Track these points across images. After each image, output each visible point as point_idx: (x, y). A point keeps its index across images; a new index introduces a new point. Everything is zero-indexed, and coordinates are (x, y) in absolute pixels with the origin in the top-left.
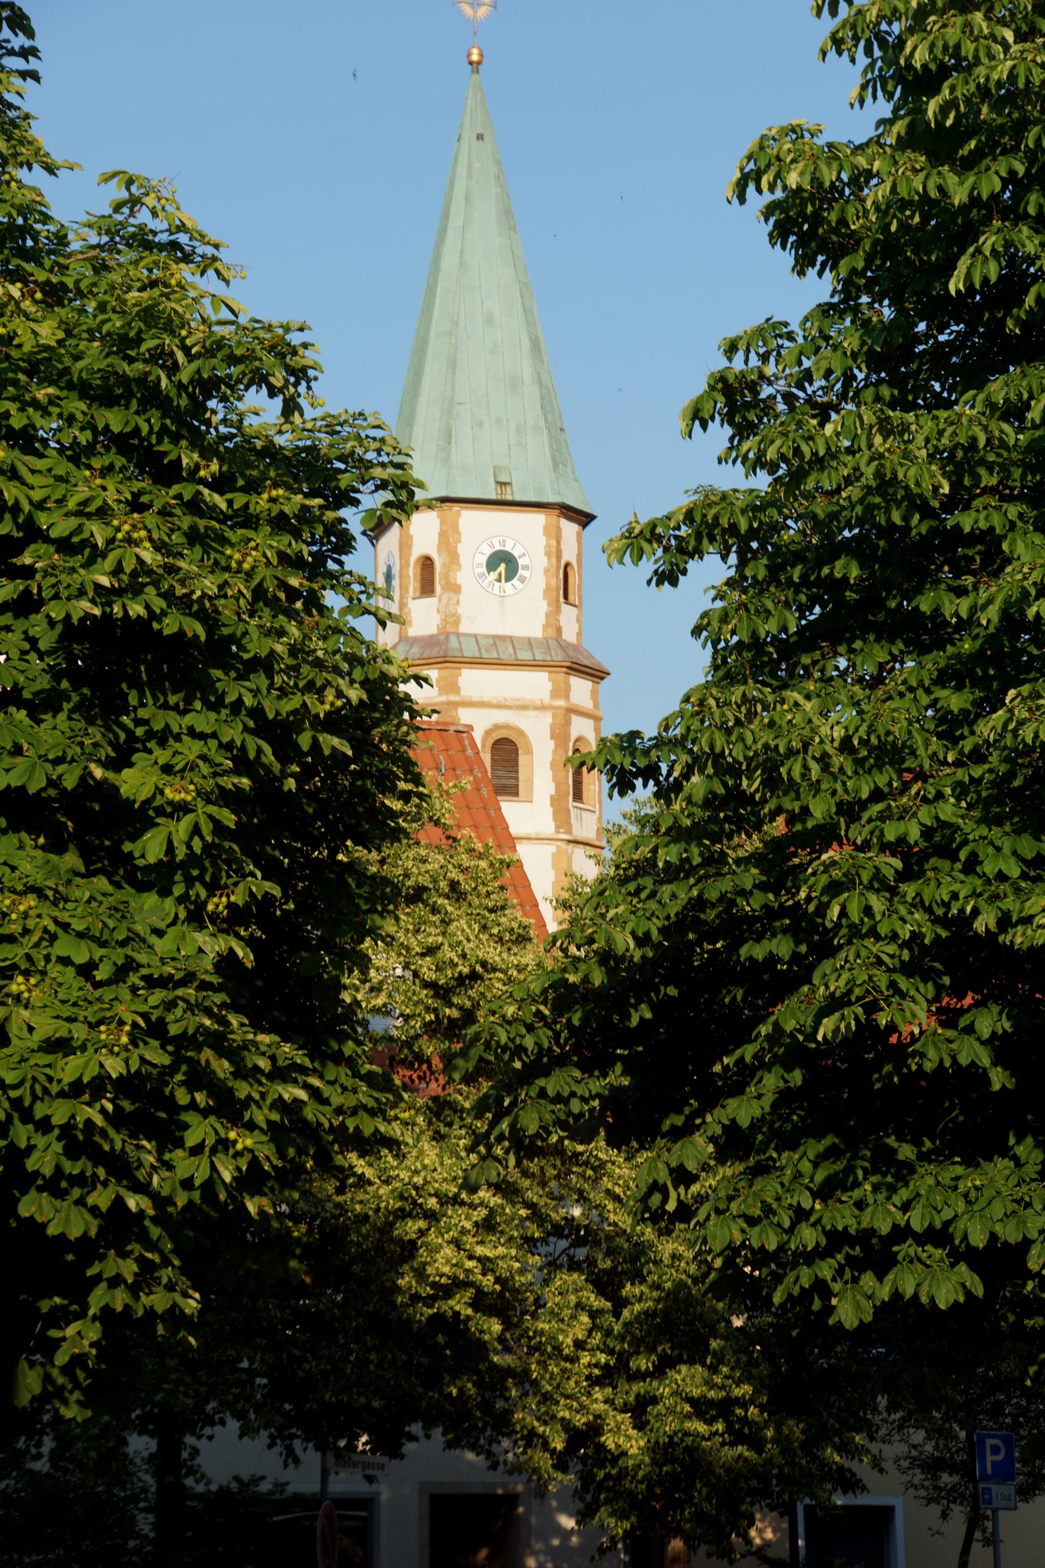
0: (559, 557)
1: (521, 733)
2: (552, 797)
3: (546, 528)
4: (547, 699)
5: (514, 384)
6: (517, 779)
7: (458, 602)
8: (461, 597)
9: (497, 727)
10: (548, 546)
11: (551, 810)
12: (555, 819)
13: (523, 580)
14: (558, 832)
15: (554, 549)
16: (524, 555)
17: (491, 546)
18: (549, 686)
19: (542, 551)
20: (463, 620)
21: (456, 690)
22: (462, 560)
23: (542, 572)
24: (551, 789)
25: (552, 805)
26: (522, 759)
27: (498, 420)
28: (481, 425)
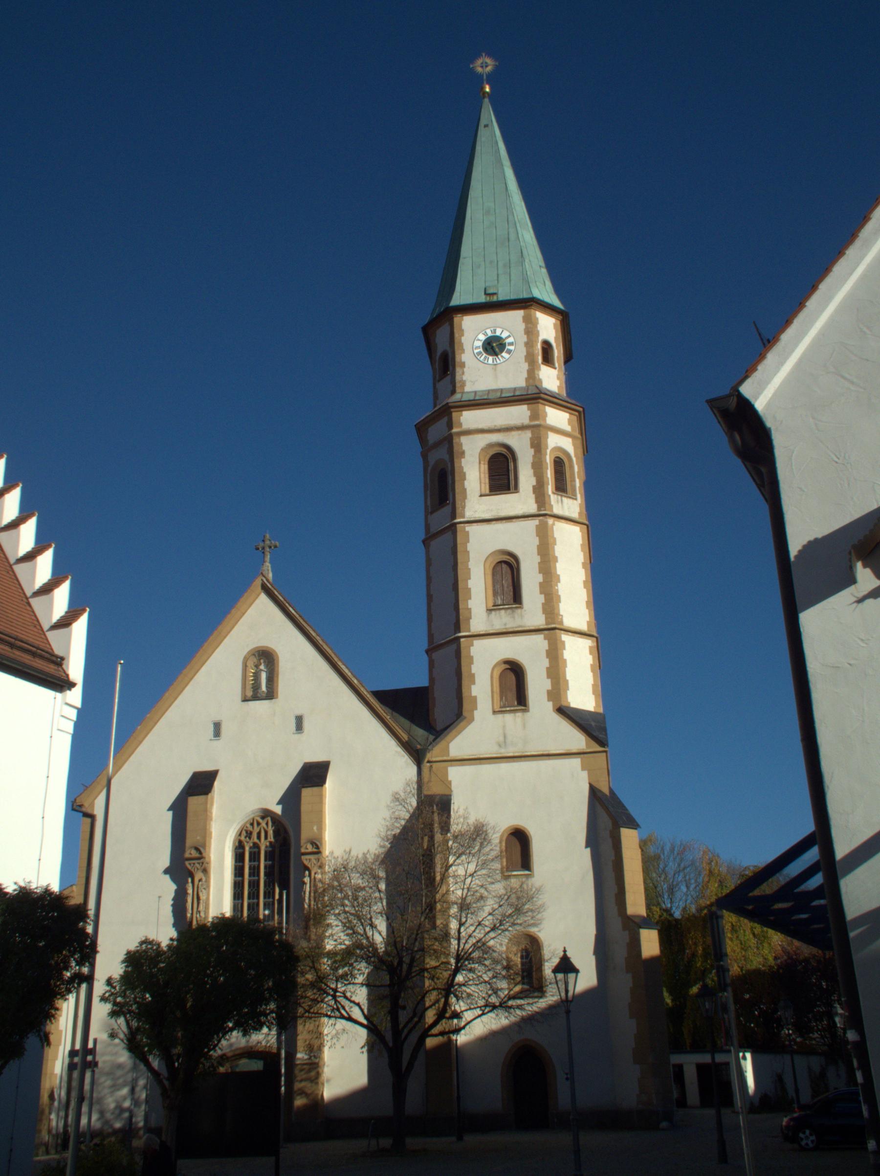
2: (534, 487)
4: (526, 421)
7: (463, 373)
8: (465, 370)
9: (491, 446)
11: (533, 496)
12: (537, 502)
13: (509, 352)
16: (509, 336)
17: (485, 334)
18: (528, 413)
19: (523, 332)
20: (467, 382)
21: (460, 425)
22: (465, 347)
23: (523, 345)
24: (533, 481)
25: (534, 492)
28: (479, 266)
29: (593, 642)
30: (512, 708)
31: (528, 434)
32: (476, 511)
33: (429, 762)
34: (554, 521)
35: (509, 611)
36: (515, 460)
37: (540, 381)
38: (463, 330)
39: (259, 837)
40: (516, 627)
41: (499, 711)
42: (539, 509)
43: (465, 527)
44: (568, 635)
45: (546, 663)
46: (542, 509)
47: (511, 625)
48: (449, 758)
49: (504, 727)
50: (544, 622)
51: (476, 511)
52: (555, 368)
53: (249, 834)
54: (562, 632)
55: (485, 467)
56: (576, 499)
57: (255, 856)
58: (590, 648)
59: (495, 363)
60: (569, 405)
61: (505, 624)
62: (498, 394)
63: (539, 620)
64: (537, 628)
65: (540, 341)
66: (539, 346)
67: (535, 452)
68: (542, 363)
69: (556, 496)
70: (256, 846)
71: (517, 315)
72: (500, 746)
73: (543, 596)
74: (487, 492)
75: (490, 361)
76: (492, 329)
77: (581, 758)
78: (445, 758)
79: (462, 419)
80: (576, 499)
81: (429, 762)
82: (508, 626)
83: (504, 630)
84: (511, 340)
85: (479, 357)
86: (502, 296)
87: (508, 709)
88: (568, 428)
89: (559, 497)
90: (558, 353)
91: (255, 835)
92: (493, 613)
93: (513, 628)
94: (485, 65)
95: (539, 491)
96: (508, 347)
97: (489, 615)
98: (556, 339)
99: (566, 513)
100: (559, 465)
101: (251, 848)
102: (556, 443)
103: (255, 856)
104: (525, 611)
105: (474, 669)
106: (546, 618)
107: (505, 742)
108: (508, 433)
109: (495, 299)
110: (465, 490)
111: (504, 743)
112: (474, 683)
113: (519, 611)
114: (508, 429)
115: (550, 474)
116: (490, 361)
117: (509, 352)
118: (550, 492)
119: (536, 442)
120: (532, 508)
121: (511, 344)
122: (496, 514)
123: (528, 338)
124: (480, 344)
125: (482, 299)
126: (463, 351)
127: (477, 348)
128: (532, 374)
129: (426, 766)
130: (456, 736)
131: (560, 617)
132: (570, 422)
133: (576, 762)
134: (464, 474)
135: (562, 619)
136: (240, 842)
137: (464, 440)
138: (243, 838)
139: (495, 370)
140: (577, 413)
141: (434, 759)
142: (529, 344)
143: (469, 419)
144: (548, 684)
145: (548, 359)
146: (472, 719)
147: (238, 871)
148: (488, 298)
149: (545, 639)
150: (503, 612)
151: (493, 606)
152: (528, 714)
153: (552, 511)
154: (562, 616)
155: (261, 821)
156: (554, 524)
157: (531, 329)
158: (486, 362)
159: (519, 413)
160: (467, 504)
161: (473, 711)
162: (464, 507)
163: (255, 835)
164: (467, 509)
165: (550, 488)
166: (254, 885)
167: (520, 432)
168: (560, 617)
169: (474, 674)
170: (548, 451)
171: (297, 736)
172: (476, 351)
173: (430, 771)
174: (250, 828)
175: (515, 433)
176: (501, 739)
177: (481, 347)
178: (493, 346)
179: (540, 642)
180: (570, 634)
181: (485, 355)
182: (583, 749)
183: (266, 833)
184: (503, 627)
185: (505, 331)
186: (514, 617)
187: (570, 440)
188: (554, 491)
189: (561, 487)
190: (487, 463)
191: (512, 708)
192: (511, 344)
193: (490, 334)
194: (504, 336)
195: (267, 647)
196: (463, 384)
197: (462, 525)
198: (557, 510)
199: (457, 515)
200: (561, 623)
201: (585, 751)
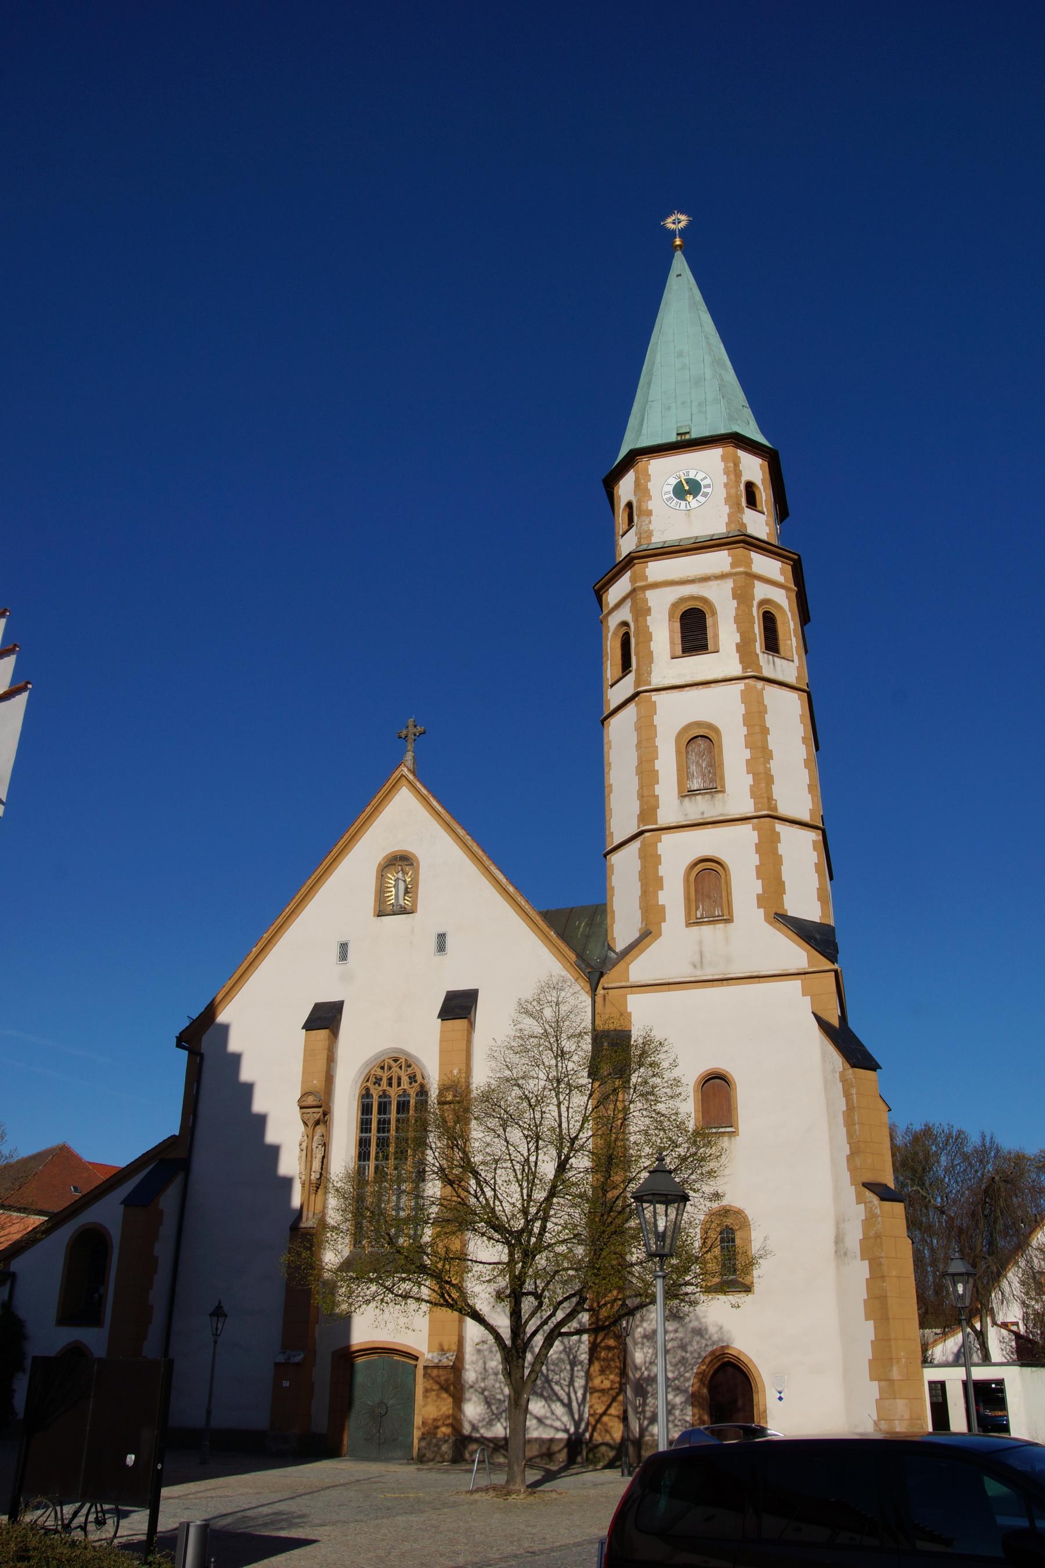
0: (738, 474)
1: (705, 600)
3: (724, 458)
4: (727, 568)
5: (698, 381)
6: (706, 639)
7: (650, 522)
8: (652, 518)
9: (682, 600)
10: (726, 467)
12: (741, 662)
13: (705, 495)
14: (743, 672)
15: (731, 469)
18: (730, 560)
20: (654, 533)
21: (646, 578)
24: (737, 639)
25: (738, 651)
26: (709, 621)
27: (683, 403)
28: (669, 408)
29: (817, 835)
30: (711, 919)
31: (729, 584)
32: (665, 677)
33: (604, 989)
34: (764, 685)
35: (708, 796)
36: (714, 613)
37: (744, 525)
38: (650, 475)
39: (390, 1085)
40: (716, 817)
41: (694, 923)
42: (744, 669)
43: (651, 696)
44: (785, 825)
45: (756, 860)
46: (749, 670)
47: (710, 815)
48: (628, 984)
49: (700, 942)
50: (753, 809)
51: (665, 677)
53: (378, 1081)
54: (776, 821)
55: (677, 625)
56: (793, 661)
57: (383, 1108)
58: (814, 842)
59: (689, 508)
60: (781, 551)
61: (703, 813)
62: (693, 541)
63: (747, 808)
64: (743, 816)
65: (743, 482)
66: (742, 487)
67: (738, 604)
68: (747, 507)
69: (766, 655)
70: (384, 1094)
71: (714, 456)
72: (695, 966)
73: (751, 776)
74: (679, 652)
75: (683, 507)
76: (684, 472)
77: (802, 980)
78: (623, 984)
79: (648, 571)
80: (793, 661)
81: (604, 989)
82: (705, 816)
83: (701, 821)
84: (707, 481)
85: (668, 504)
86: (695, 435)
87: (706, 920)
88: (781, 579)
89: (771, 657)
90: (765, 495)
91: (384, 1082)
92: (687, 799)
93: (713, 817)
94: (677, 222)
95: (744, 649)
96: (703, 490)
97: (681, 803)
98: (762, 480)
99: (780, 677)
100: (769, 621)
101: (380, 1097)
102: (765, 594)
103: (383, 1108)
104: (728, 795)
105: (662, 871)
106: (755, 804)
107: (701, 962)
108: (705, 584)
109: (687, 437)
110: (652, 652)
111: (700, 962)
112: (661, 888)
113: (720, 795)
114: (706, 579)
115: (758, 629)
116: (683, 507)
117: (705, 495)
118: (758, 651)
119: (739, 592)
120: (737, 670)
121: (708, 486)
122: (690, 679)
123: (727, 479)
124: (671, 488)
125: (673, 438)
126: (650, 497)
127: (667, 493)
128: (735, 515)
129: (600, 992)
130: (638, 955)
131: (774, 802)
132: (782, 572)
133: (796, 984)
134: (651, 634)
135: (776, 805)
136: (368, 1089)
137: (649, 594)
138: (369, 1084)
139: (689, 516)
141: (610, 986)
143: (656, 570)
144: (757, 887)
145: (752, 501)
146: (660, 935)
147: (364, 1126)
148: (679, 438)
149: (754, 829)
150: (699, 797)
151: (689, 791)
152: (730, 926)
153: (762, 673)
154: (776, 801)
155: (393, 1063)
156: (764, 689)
159: (720, 560)
160: (653, 669)
161: (660, 923)
162: (650, 673)
163: (384, 1082)
164: (653, 675)
165: (759, 645)
166: (383, 1143)
167: (719, 582)
168: (774, 802)
169: (662, 877)
170: (755, 603)
171: (438, 958)
172: (664, 497)
173: (604, 999)
174: (379, 1072)
175: (713, 584)
176: (697, 958)
177: (671, 492)
178: (686, 489)
179: (747, 833)
180: (787, 823)
181: (676, 500)
182: (804, 969)
183: (399, 1079)
184: (701, 817)
186: (714, 804)
187: (783, 592)
188: (764, 650)
189: (772, 645)
190: (679, 620)
191: (711, 919)
192: (708, 486)
194: (698, 478)
195: (406, 851)
197: (648, 694)
198: (767, 673)
199: (641, 683)
200: (775, 809)
201: (807, 970)
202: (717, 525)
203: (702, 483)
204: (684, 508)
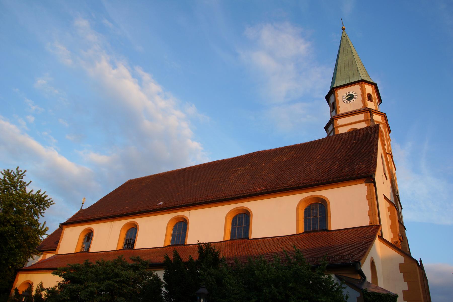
13: (355, 98)
52: (373, 102)
65: (366, 93)
66: (366, 95)
71: (358, 87)
90: (374, 96)
96: (355, 97)
98: (373, 93)
117: (355, 98)
121: (356, 96)
132: (381, 119)
140: (383, 116)
142: (363, 95)
157: (363, 90)
158: (347, 103)
178: (350, 97)
185: (353, 92)
192: (356, 96)
193: (348, 94)
196: (340, 111)
202: (360, 106)
203: (354, 95)
204: (349, 103)
